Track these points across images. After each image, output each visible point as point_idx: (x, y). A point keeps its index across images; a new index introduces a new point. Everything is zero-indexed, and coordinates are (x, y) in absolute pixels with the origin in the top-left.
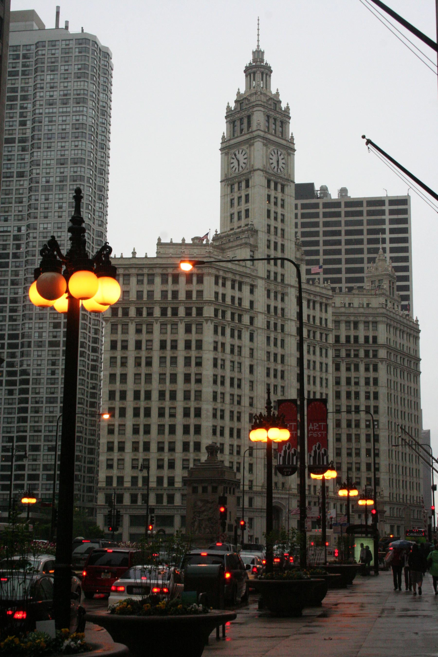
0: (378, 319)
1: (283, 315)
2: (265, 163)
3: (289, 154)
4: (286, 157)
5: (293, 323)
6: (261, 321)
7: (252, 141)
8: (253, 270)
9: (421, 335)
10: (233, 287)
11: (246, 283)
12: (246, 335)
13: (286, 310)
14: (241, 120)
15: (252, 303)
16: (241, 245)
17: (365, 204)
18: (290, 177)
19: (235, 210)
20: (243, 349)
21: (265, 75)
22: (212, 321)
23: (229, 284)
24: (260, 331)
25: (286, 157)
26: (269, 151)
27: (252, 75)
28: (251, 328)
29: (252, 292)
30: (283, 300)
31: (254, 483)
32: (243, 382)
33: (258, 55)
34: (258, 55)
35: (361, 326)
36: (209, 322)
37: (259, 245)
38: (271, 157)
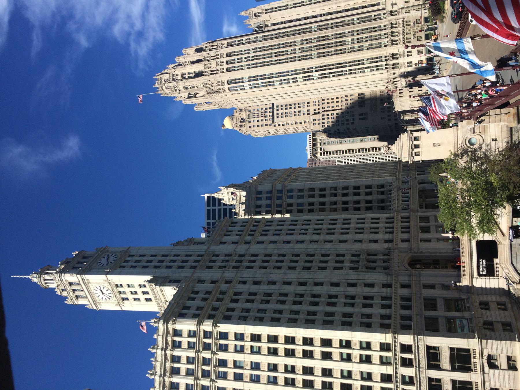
0: (254, 190)
1: (230, 255)
3: (107, 251)
5: (239, 247)
6: (229, 274)
7: (86, 281)
9: (274, 169)
10: (193, 299)
12: (241, 288)
13: (227, 253)
14: (74, 290)
15: (213, 282)
16: (162, 292)
17: (209, 221)
19: (142, 297)
20: (251, 291)
21: (48, 272)
24: (239, 275)
27: (46, 282)
29: (203, 282)
30: (218, 256)
31: (385, 282)
32: (282, 292)
35: (259, 203)
36: (218, 325)
37: (166, 275)
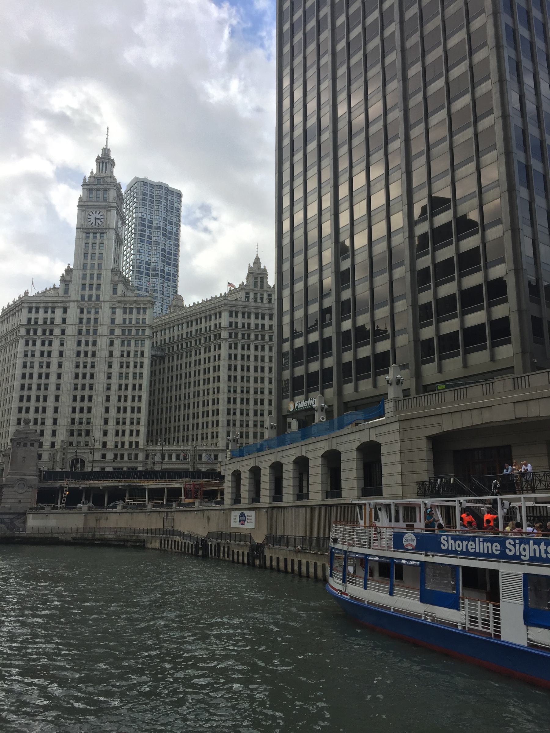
2: (83, 223)
3: (110, 211)
4: (105, 214)
5: (107, 327)
6: (71, 331)
8: (66, 298)
11: (59, 307)
18: (109, 225)
22: (22, 338)
23: (41, 311)
25: (105, 214)
26: (87, 213)
28: (62, 336)
33: (106, 152)
34: (106, 152)
38: (89, 217)
